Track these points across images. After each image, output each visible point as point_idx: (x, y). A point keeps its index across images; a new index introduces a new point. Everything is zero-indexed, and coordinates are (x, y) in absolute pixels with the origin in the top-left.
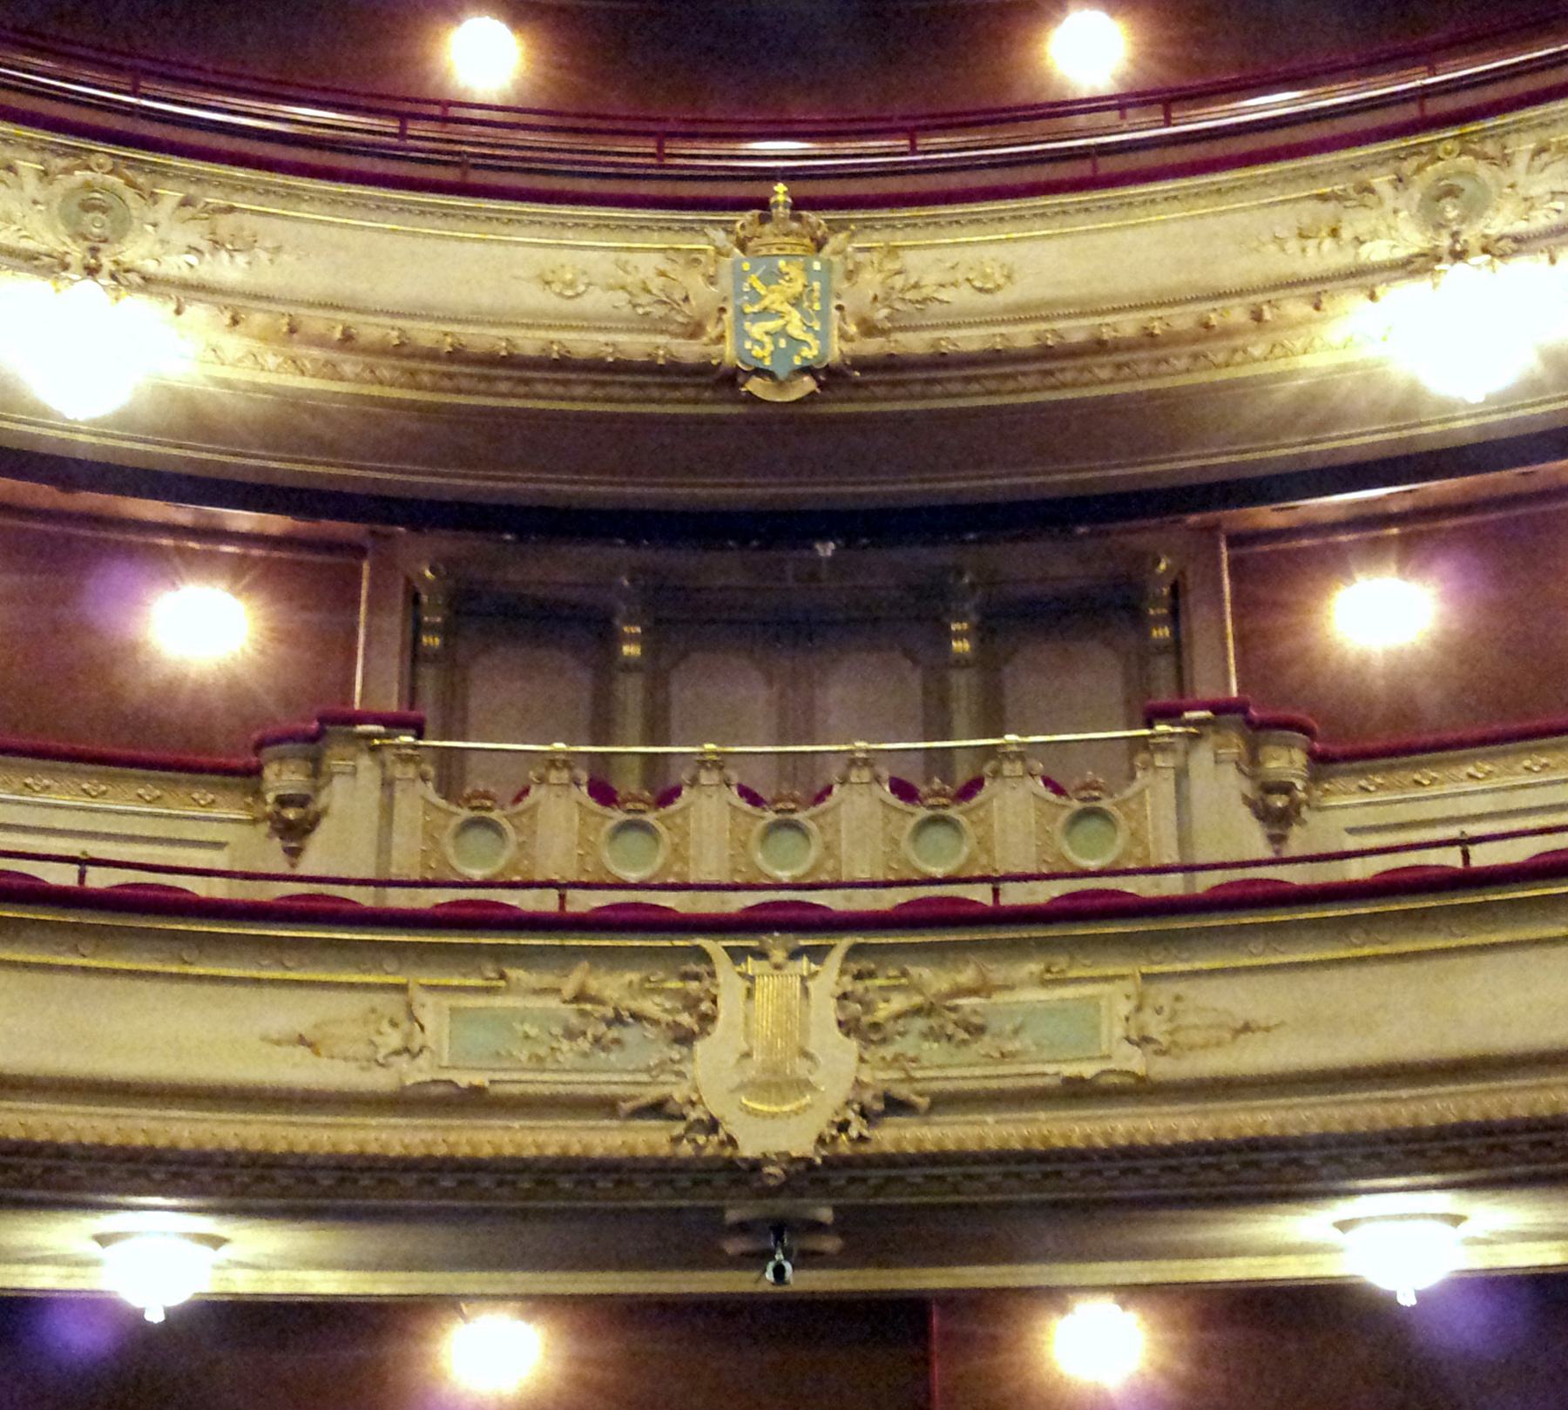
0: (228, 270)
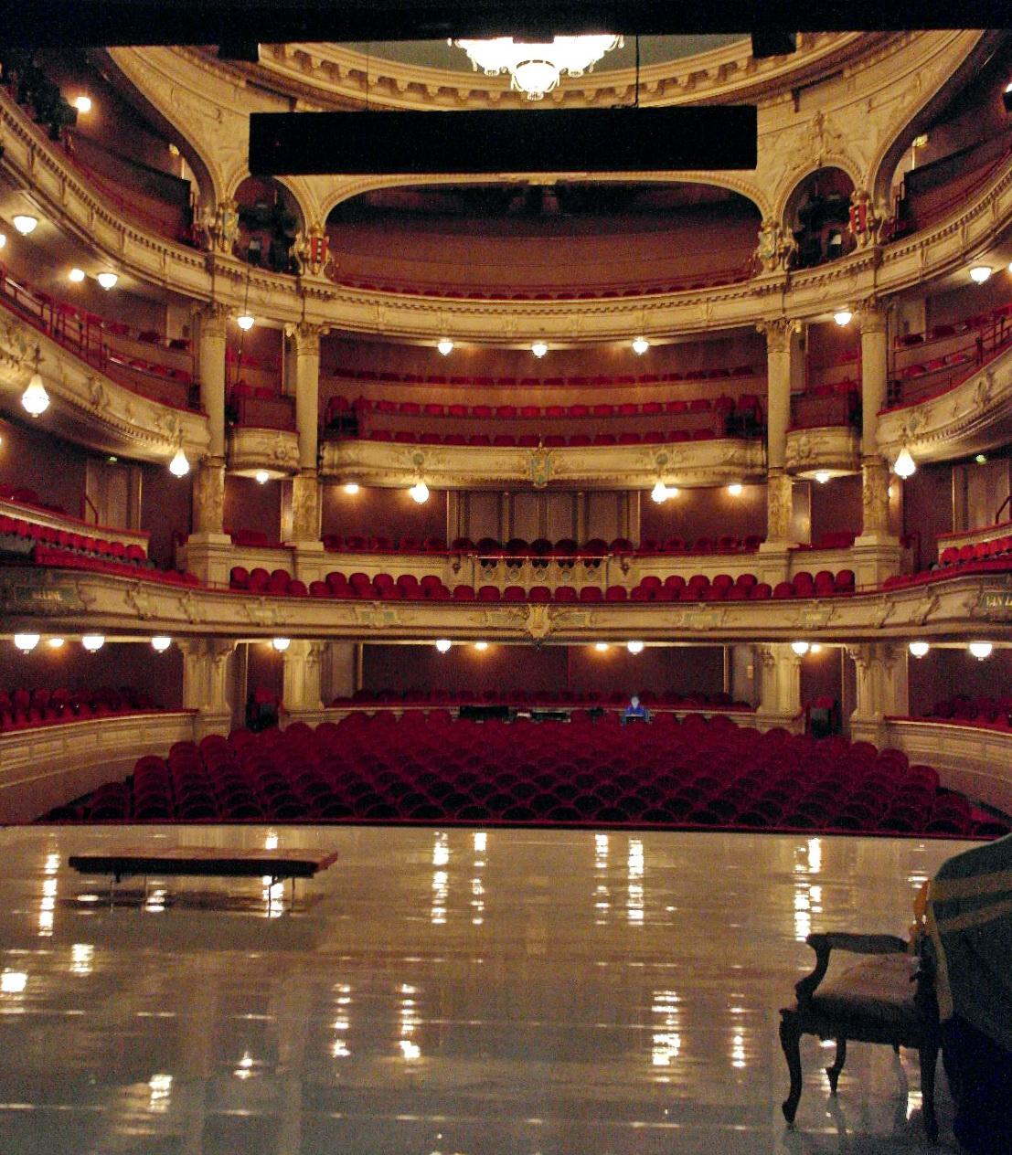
0: (441, 467)
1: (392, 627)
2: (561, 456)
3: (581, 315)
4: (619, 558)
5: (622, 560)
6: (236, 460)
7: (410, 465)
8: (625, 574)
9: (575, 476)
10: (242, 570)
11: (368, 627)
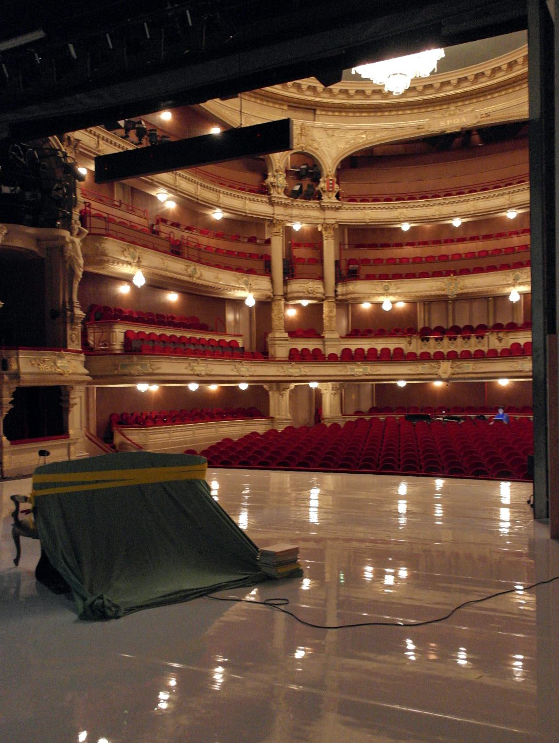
0: (399, 291)
1: (301, 376)
2: (463, 280)
3: (476, 201)
4: (495, 334)
5: (498, 334)
6: (289, 296)
7: (382, 291)
9: (471, 290)
10: (296, 350)
11: (353, 375)
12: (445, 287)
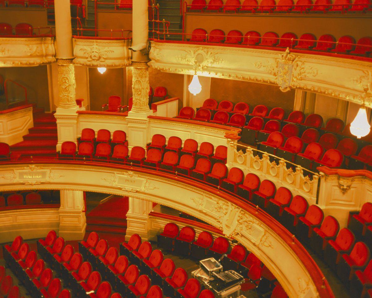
0: (215, 65)
5: (339, 179)
8: (344, 193)
12: (276, 70)
